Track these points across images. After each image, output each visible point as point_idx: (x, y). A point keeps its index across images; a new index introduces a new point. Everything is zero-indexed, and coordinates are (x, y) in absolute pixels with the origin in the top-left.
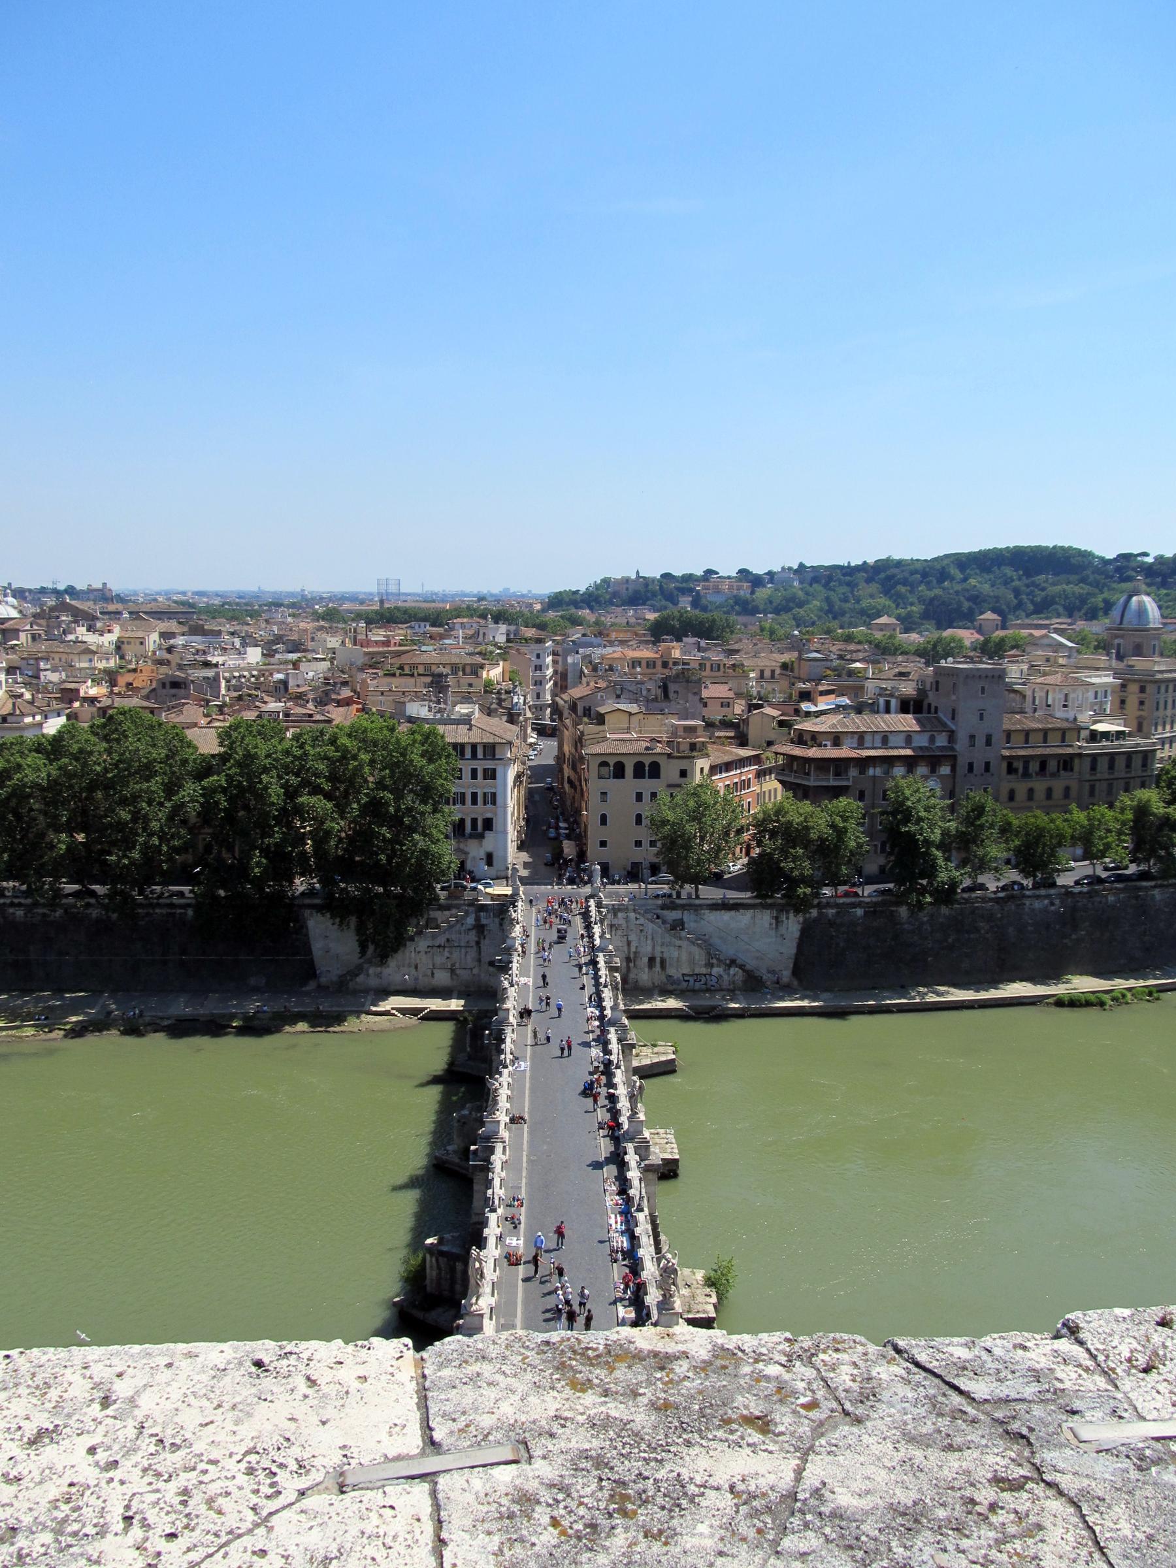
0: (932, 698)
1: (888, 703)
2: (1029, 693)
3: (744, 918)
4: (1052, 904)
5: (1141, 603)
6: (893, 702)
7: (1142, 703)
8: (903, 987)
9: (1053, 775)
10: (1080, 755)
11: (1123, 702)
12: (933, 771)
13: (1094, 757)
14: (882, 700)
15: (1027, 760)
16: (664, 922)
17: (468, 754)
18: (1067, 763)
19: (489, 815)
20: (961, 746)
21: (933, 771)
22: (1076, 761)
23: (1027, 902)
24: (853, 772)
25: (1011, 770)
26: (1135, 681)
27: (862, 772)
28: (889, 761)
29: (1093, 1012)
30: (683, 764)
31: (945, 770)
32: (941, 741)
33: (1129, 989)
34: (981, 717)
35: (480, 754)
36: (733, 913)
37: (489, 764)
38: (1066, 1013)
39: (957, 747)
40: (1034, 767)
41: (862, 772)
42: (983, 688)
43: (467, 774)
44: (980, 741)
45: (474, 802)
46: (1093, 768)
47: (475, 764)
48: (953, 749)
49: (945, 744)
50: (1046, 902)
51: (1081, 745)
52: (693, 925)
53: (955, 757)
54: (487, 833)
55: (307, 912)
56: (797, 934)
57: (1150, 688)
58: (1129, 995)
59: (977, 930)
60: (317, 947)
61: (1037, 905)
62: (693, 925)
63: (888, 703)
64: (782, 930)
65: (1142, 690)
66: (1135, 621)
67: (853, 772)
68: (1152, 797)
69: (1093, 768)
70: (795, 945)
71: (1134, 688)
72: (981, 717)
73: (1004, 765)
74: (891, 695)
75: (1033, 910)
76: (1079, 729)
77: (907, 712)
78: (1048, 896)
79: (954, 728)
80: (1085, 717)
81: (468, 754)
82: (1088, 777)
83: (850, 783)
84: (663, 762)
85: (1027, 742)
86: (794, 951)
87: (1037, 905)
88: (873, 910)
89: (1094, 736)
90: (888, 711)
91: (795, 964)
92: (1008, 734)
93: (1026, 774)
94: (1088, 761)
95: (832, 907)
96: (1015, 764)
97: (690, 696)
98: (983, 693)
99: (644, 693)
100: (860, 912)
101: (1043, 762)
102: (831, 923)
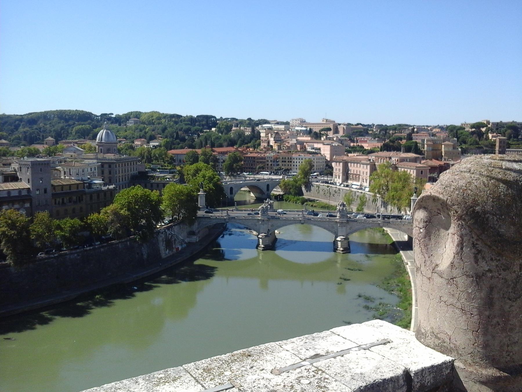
46: (91, 198)
65: (110, 166)
69: (91, 198)
71: (106, 166)
98: (41, 171)
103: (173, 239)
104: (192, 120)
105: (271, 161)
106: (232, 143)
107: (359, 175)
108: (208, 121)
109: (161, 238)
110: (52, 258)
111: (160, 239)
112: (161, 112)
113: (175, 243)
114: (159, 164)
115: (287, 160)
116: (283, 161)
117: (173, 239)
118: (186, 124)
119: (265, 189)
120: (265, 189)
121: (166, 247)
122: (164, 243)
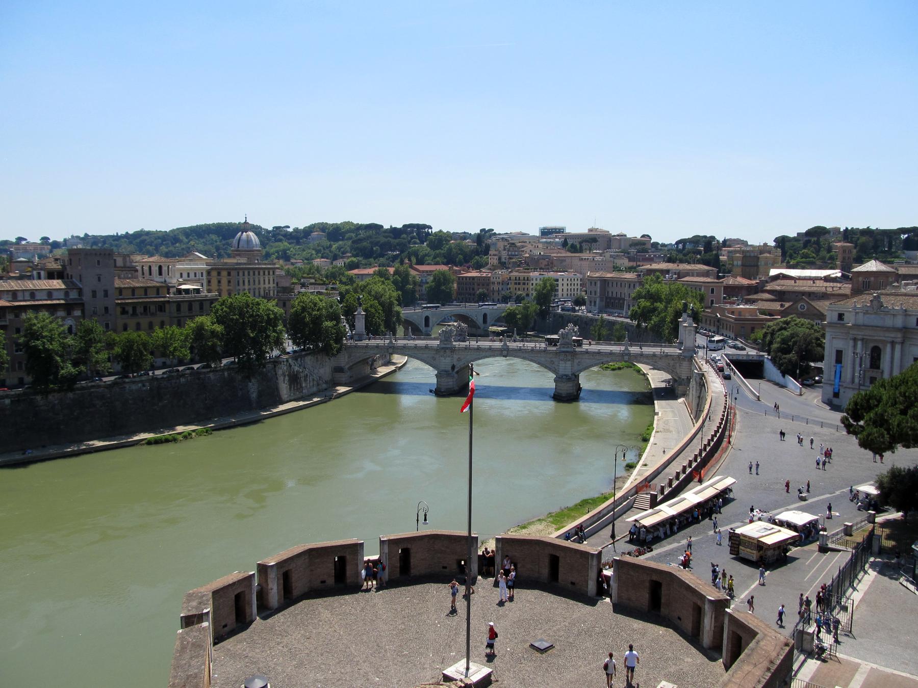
0: (69, 271)
1: (39, 274)
2: (139, 268)
4: (144, 386)
5: (247, 236)
6: (42, 273)
7: (229, 282)
8: (44, 447)
9: (152, 314)
10: (168, 302)
12: (69, 314)
13: (179, 304)
14: (35, 273)
15: (134, 306)
18: (161, 307)
20: (87, 297)
21: (69, 314)
22: (167, 306)
23: (127, 386)
25: (124, 312)
26: (224, 269)
28: (36, 308)
29: (170, 446)
31: (77, 313)
32: (73, 295)
33: (194, 431)
34: (99, 279)
38: (153, 448)
39: (84, 298)
40: (140, 310)
41: (17, 316)
42: (98, 262)
44: (100, 294)
46: (179, 309)
48: (82, 299)
49: (77, 297)
50: (140, 385)
51: (171, 297)
57: (233, 273)
58: (194, 434)
61: (134, 387)
63: (39, 274)
65: (229, 274)
66: (245, 246)
67: (10, 316)
68: (206, 321)
69: (179, 309)
71: (224, 273)
72: (99, 279)
73: (119, 309)
74: (41, 269)
76: (168, 288)
77: (53, 278)
78: (141, 381)
79: (81, 286)
80: (174, 281)
82: (176, 315)
83: (8, 323)
85: (133, 294)
87: (134, 387)
88: (17, 400)
89: (179, 291)
90: (39, 278)
92: (120, 290)
93: (135, 313)
94: (175, 305)
96: (127, 308)
100: (7, 401)
101: (146, 307)
103: (302, 375)
104: (394, 231)
105: (499, 283)
106: (450, 260)
107: (624, 300)
108: (418, 231)
109: (282, 369)
111: (280, 372)
112: (355, 223)
113: (306, 380)
114: (310, 278)
115: (522, 282)
116: (516, 284)
117: (302, 375)
118: (386, 237)
119: (480, 321)
120: (480, 321)
121: (290, 385)
122: (287, 378)
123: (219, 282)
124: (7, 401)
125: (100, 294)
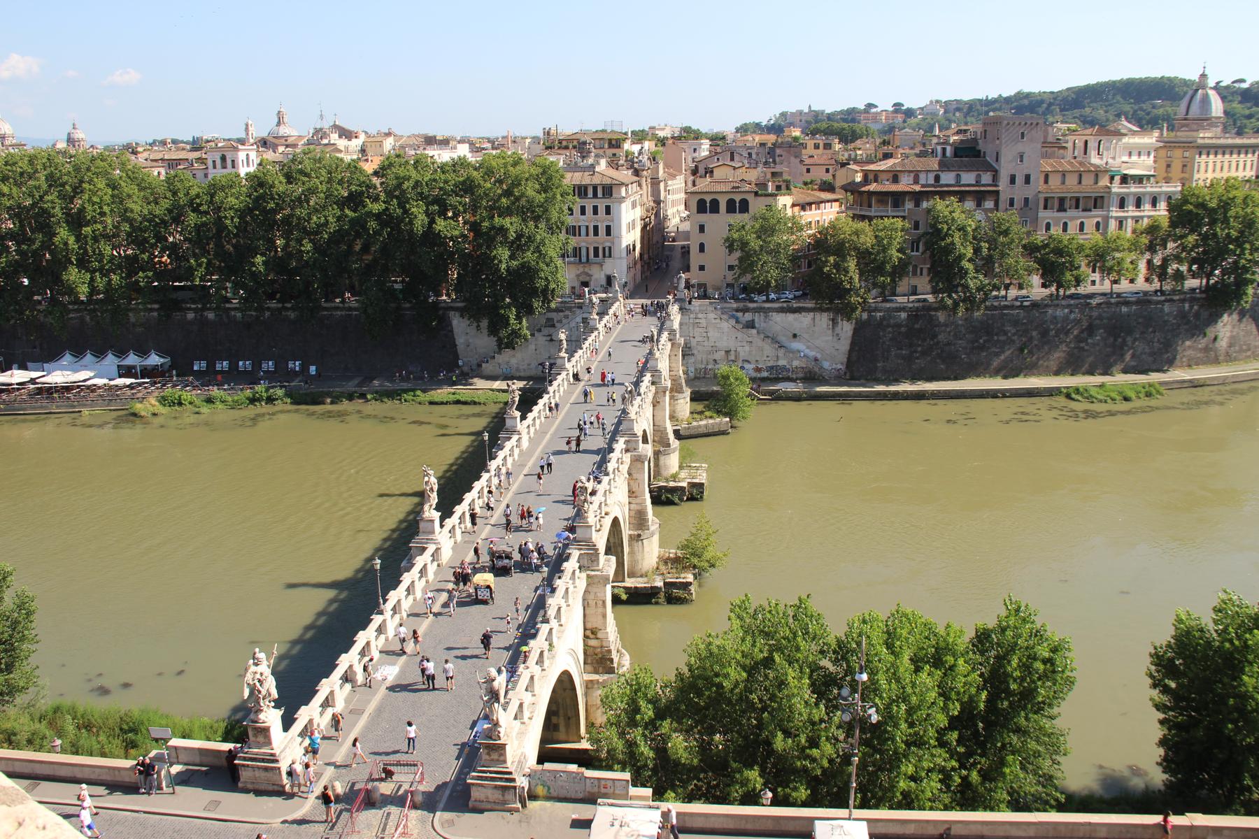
2: (1070, 145)
3: (805, 320)
11: (1168, 166)
12: (979, 205)
14: (939, 148)
16: (737, 322)
17: (590, 194)
19: (608, 244)
24: (909, 205)
27: (917, 205)
30: (769, 200)
31: (989, 204)
35: (600, 194)
36: (796, 315)
37: (607, 202)
41: (917, 205)
43: (589, 210)
44: (1020, 180)
45: (596, 233)
47: (595, 202)
52: (763, 325)
53: (997, 192)
54: (607, 260)
55: (452, 313)
56: (850, 333)
59: (1005, 333)
60: (460, 341)
62: (763, 325)
64: (838, 330)
67: (909, 205)
70: (849, 342)
75: (1055, 318)
81: (590, 194)
84: (750, 198)
86: (847, 347)
91: (849, 359)
95: (880, 311)
97: (792, 159)
99: (754, 156)
100: (903, 315)
102: (881, 325)
110: (1018, 307)
123: (1168, 166)
124: (903, 315)
125: (1020, 180)
